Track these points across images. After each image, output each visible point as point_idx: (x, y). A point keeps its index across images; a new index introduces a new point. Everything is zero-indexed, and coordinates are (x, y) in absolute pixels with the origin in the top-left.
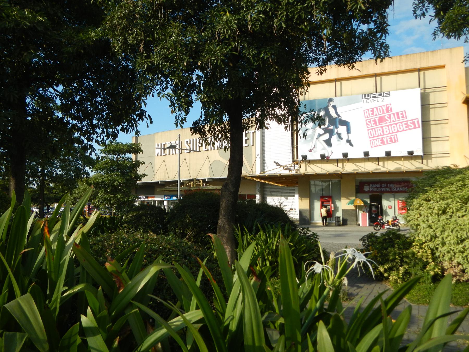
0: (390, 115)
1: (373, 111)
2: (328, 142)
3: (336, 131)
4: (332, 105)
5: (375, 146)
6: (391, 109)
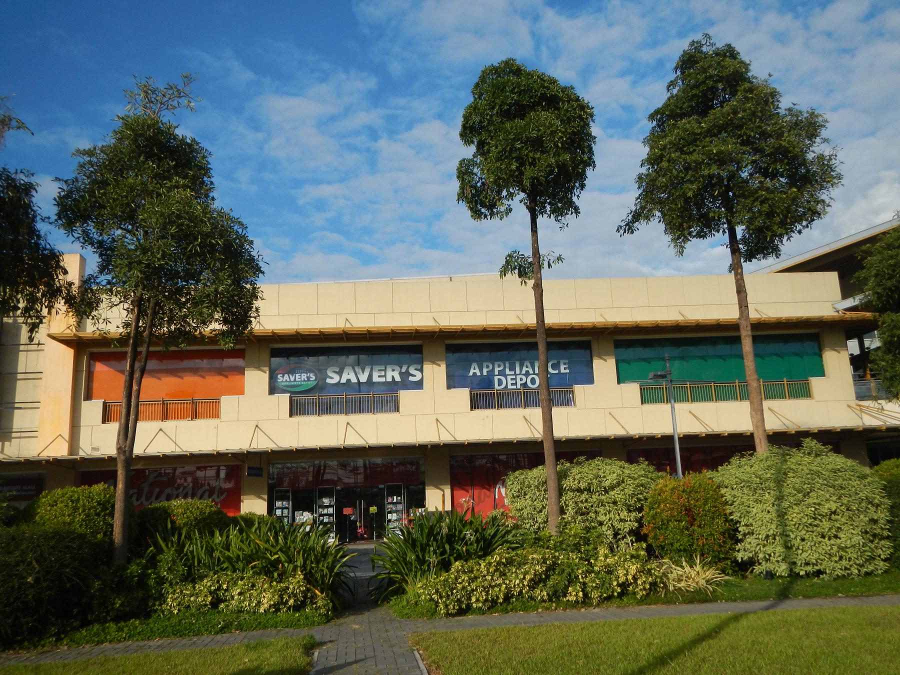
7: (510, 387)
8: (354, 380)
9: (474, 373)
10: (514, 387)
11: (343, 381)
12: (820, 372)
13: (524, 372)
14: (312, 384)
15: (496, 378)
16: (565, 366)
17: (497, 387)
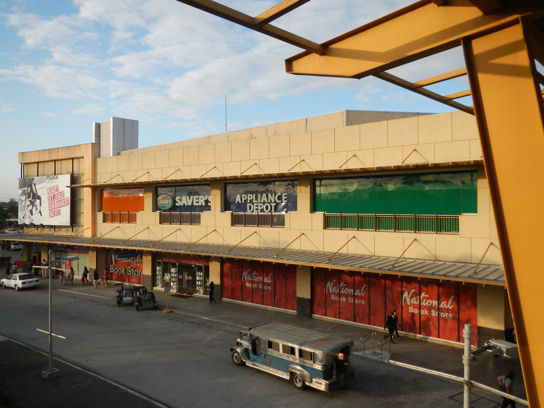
0: (58, 193)
1: (51, 189)
2: (31, 211)
3: (35, 203)
4: (34, 183)
5: (51, 217)
6: (58, 189)
8: (186, 205)
10: (257, 211)
11: (182, 205)
12: (473, 208)
13: (262, 201)
14: (169, 206)
15: (248, 205)
16: (286, 197)
17: (248, 210)
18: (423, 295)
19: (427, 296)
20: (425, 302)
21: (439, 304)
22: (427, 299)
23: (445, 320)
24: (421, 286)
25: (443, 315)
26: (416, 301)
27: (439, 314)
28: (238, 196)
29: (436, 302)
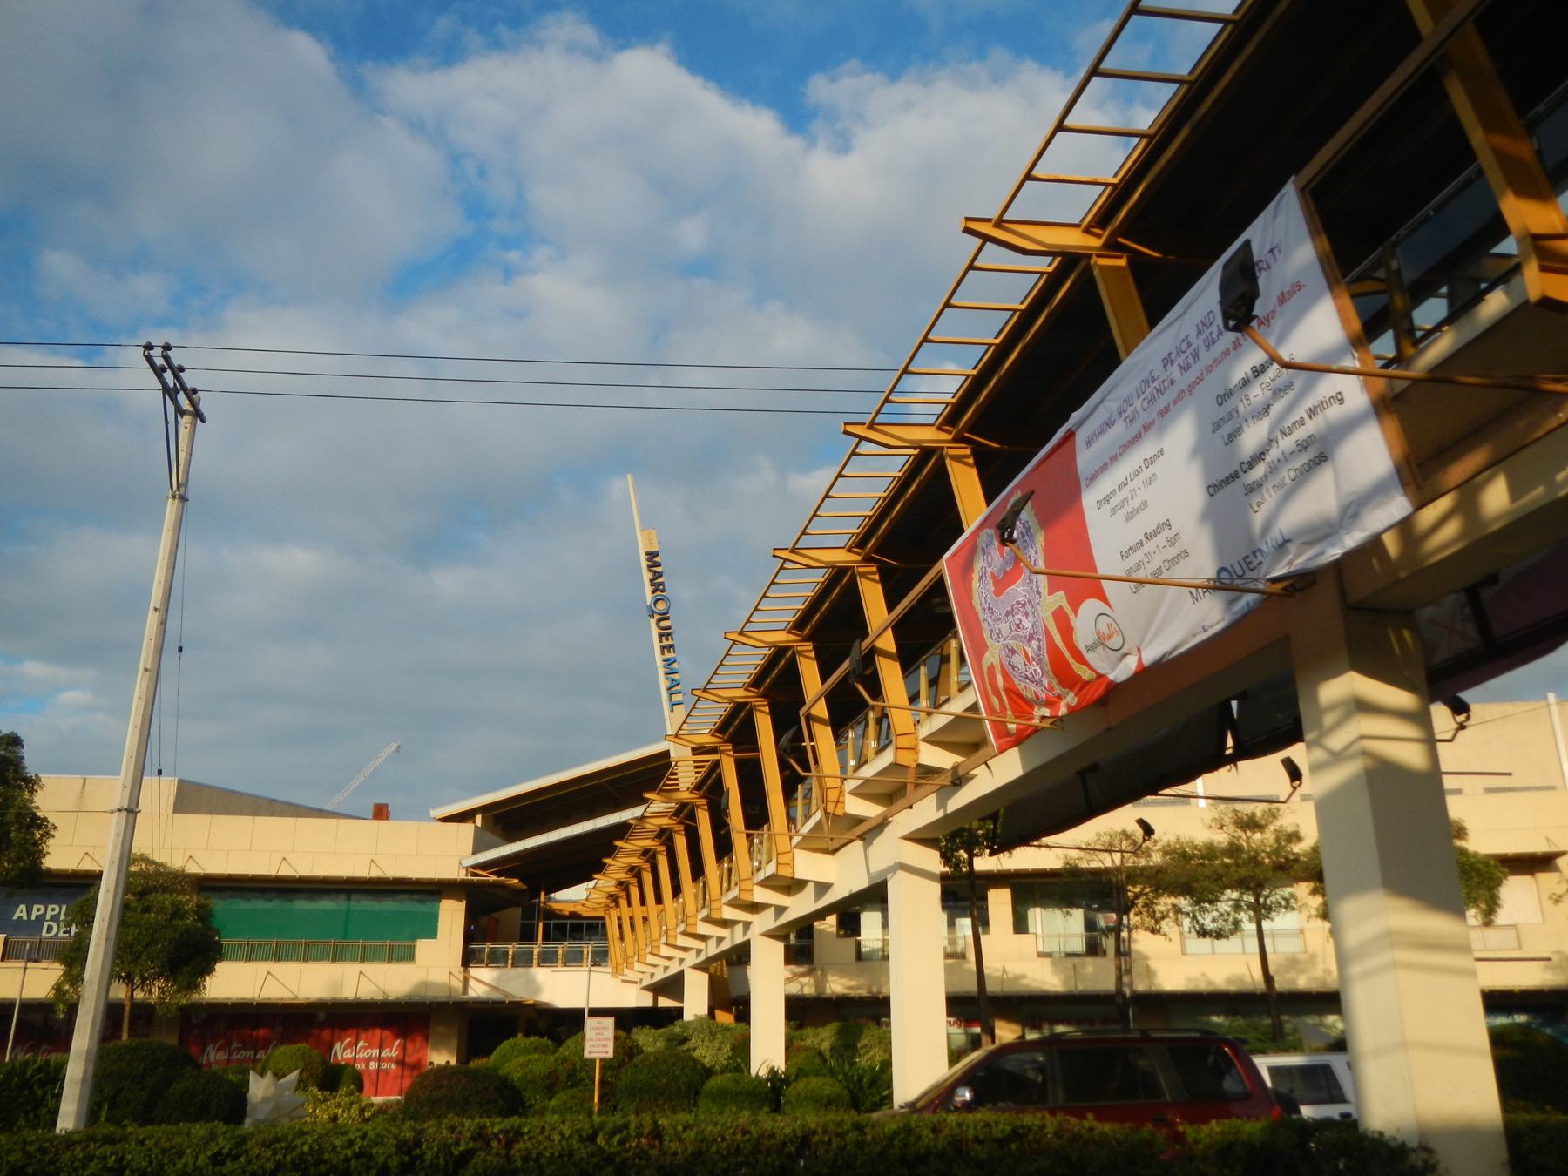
7: (61, 935)
9: (20, 917)
10: (67, 935)
12: (432, 934)
15: (46, 925)
17: (44, 934)
18: (361, 1044)
19: (366, 1044)
20: (363, 1053)
21: (380, 1053)
22: (365, 1048)
23: (387, 1072)
24: (360, 1030)
25: (384, 1066)
26: (351, 1053)
27: (379, 1066)
28: (23, 907)
29: (378, 1051)
